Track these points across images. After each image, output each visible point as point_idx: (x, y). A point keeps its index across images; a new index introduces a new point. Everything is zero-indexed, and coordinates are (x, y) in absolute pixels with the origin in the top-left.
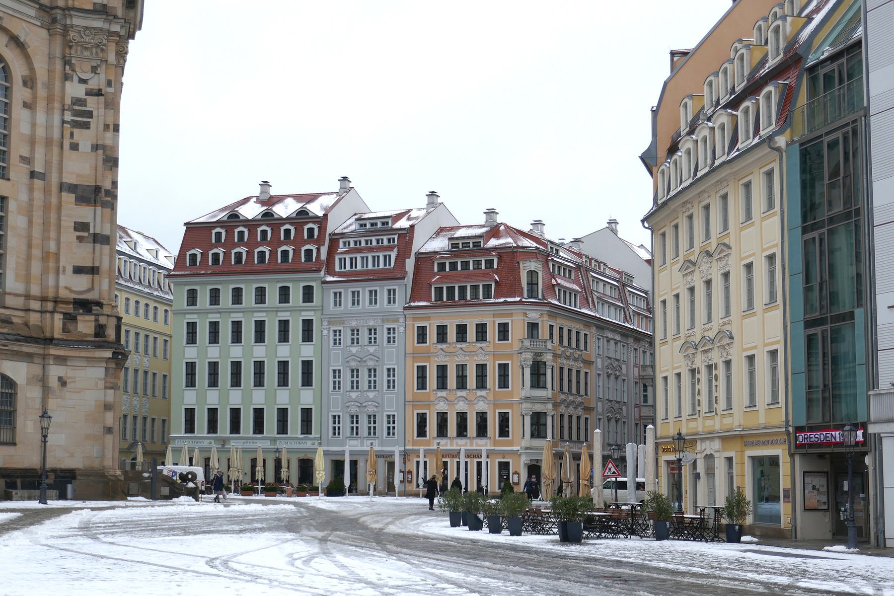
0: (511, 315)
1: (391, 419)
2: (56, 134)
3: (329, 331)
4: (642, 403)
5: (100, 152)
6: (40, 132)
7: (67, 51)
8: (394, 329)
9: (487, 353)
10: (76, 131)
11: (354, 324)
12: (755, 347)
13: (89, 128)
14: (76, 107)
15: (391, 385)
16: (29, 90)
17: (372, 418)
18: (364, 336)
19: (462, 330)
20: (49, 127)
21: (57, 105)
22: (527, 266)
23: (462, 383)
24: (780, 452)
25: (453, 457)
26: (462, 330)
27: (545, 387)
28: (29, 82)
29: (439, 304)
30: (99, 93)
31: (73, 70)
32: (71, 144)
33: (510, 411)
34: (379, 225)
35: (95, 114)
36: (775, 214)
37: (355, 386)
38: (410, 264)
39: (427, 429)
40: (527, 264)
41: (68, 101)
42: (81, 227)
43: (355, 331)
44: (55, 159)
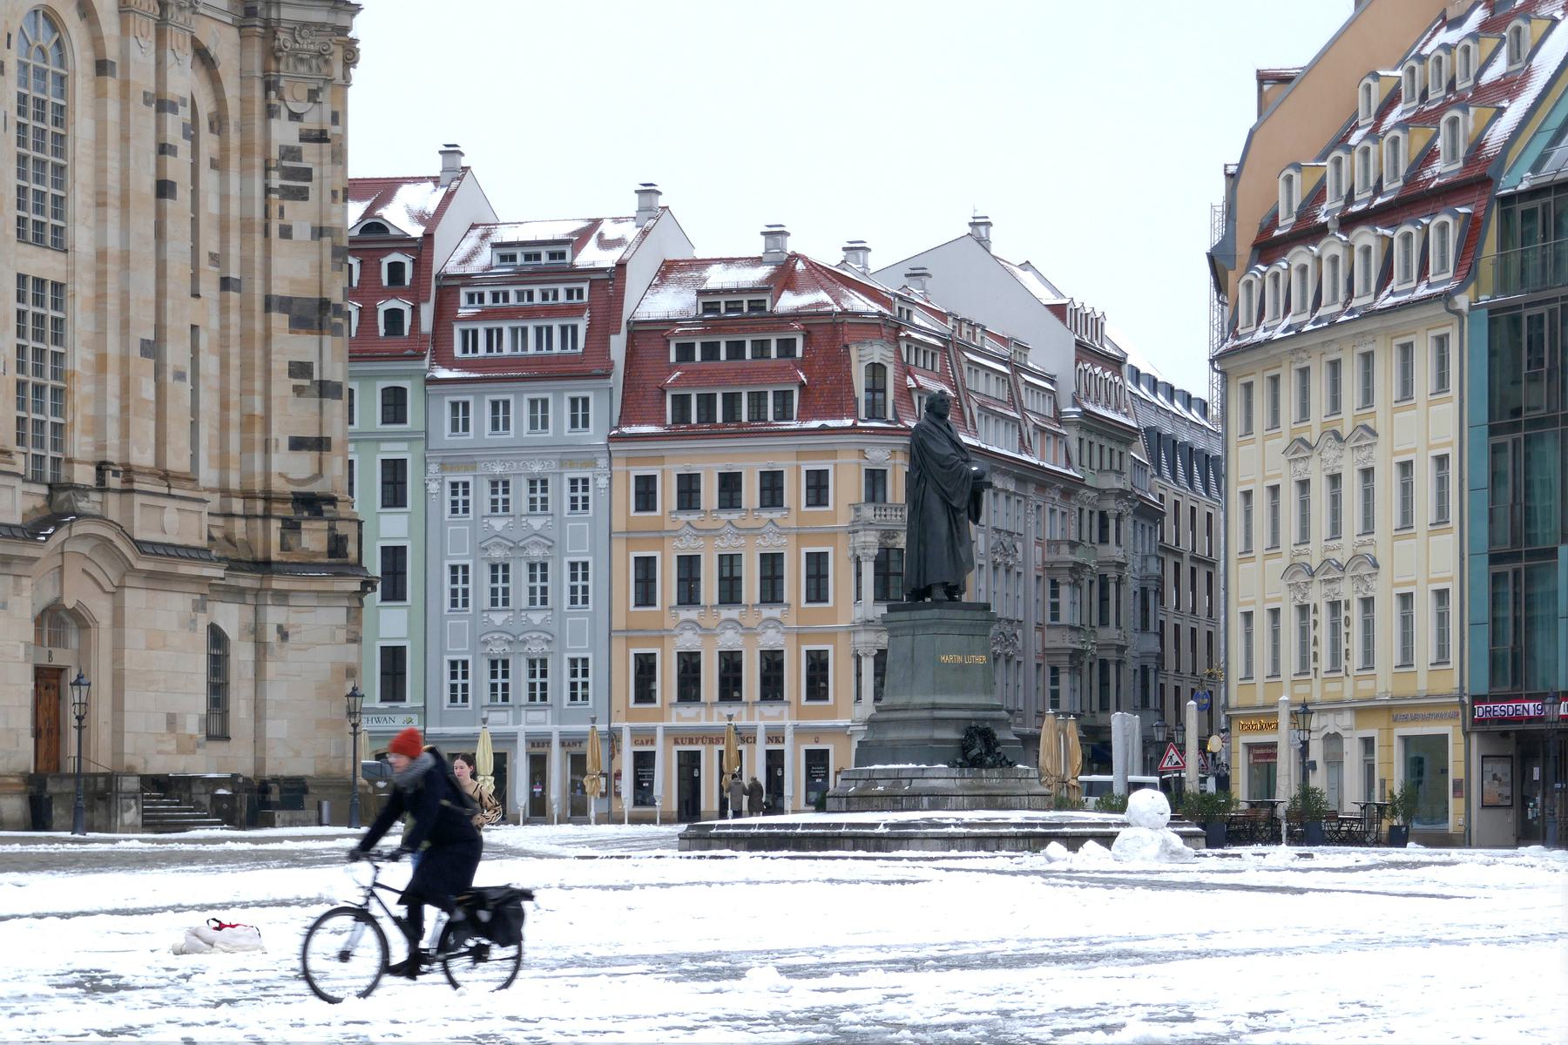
0: (832, 454)
1: (579, 667)
2: (258, 213)
3: (442, 484)
4: (1048, 621)
5: (327, 240)
6: (234, 209)
7: (273, 66)
8: (585, 481)
9: (785, 532)
10: (287, 204)
11: (498, 470)
12: (1414, 583)
13: (306, 199)
14: (286, 163)
15: (579, 596)
16: (215, 137)
17: (539, 667)
18: (520, 495)
19: (730, 485)
20: (245, 199)
21: (258, 161)
22: (863, 356)
23: (730, 592)
24: (1451, 729)
25: (711, 741)
26: (730, 485)
28: (218, 123)
29: (681, 429)
30: (321, 137)
31: (281, 99)
32: (281, 227)
33: (830, 648)
34: (545, 259)
35: (315, 173)
36: (1450, 399)
37: (500, 599)
38: (618, 345)
39: (658, 686)
40: (867, 350)
41: (275, 154)
42: (300, 369)
43: (500, 485)
44: (258, 254)
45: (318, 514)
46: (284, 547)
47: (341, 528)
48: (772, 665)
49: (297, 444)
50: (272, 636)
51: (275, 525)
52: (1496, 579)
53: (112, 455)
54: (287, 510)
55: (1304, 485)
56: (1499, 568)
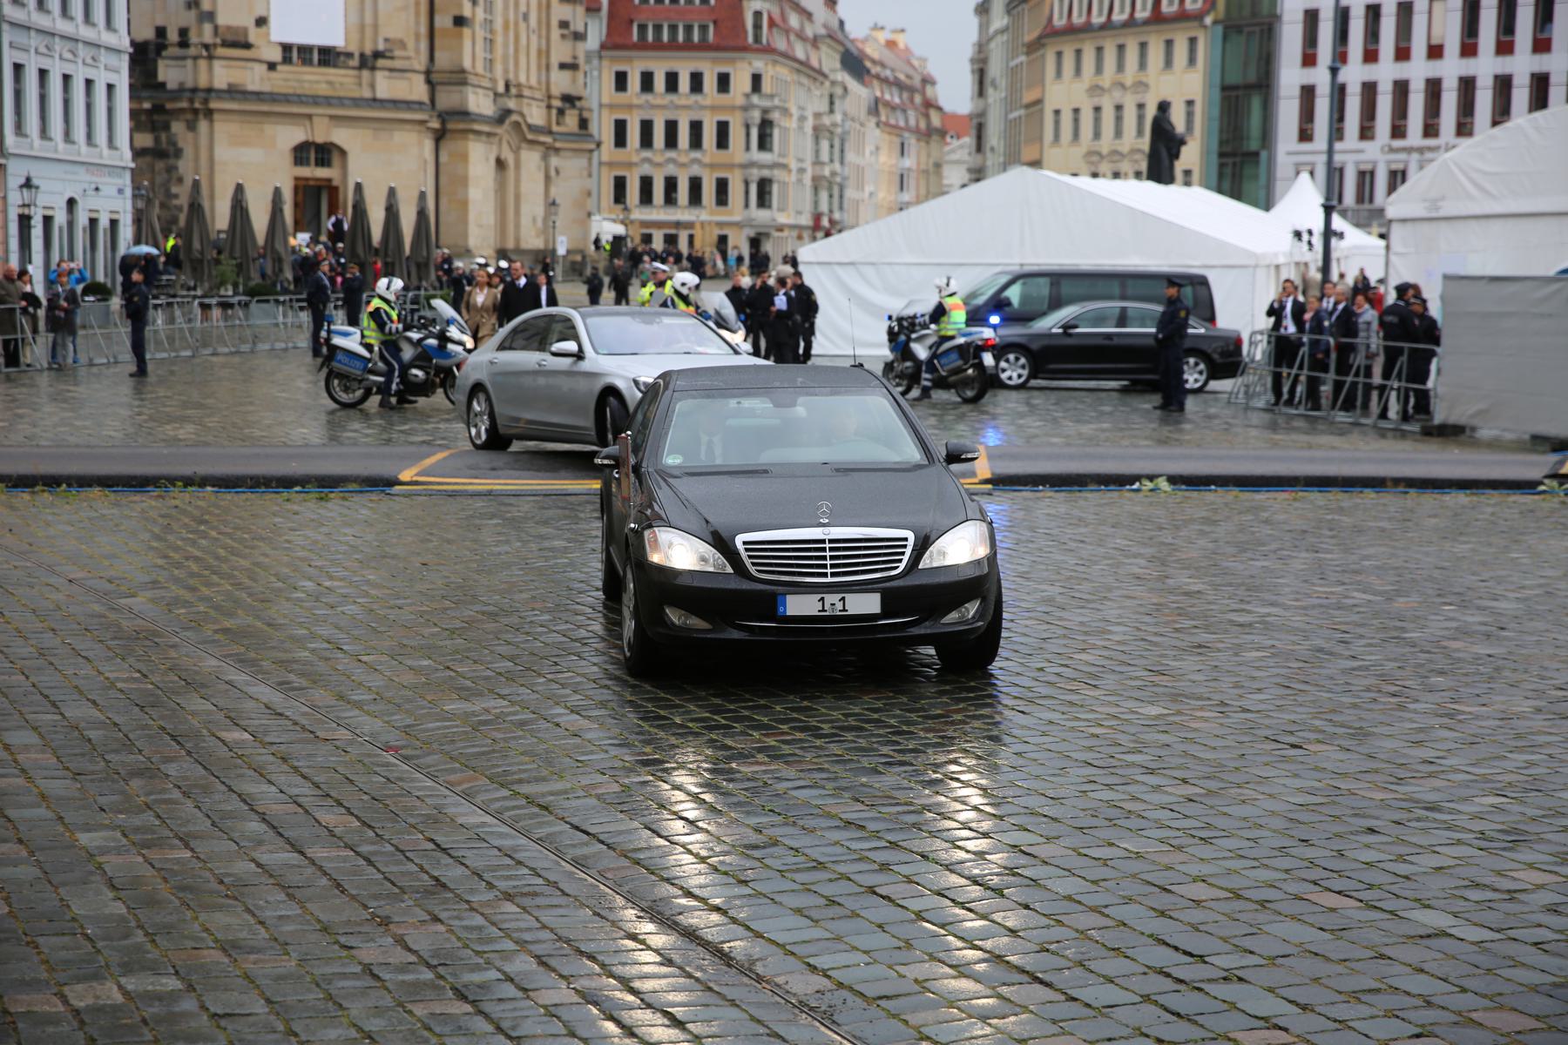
19: (672, 82)
23: (671, 141)
27: (771, 150)
29: (643, 45)
42: (564, 24)
45: (574, 106)
46: (558, 124)
47: (586, 114)
48: (696, 185)
49: (563, 66)
50: (553, 173)
51: (554, 112)
52: (1222, 166)
53: (511, 76)
54: (557, 103)
55: (1097, 109)
56: (1225, 160)
